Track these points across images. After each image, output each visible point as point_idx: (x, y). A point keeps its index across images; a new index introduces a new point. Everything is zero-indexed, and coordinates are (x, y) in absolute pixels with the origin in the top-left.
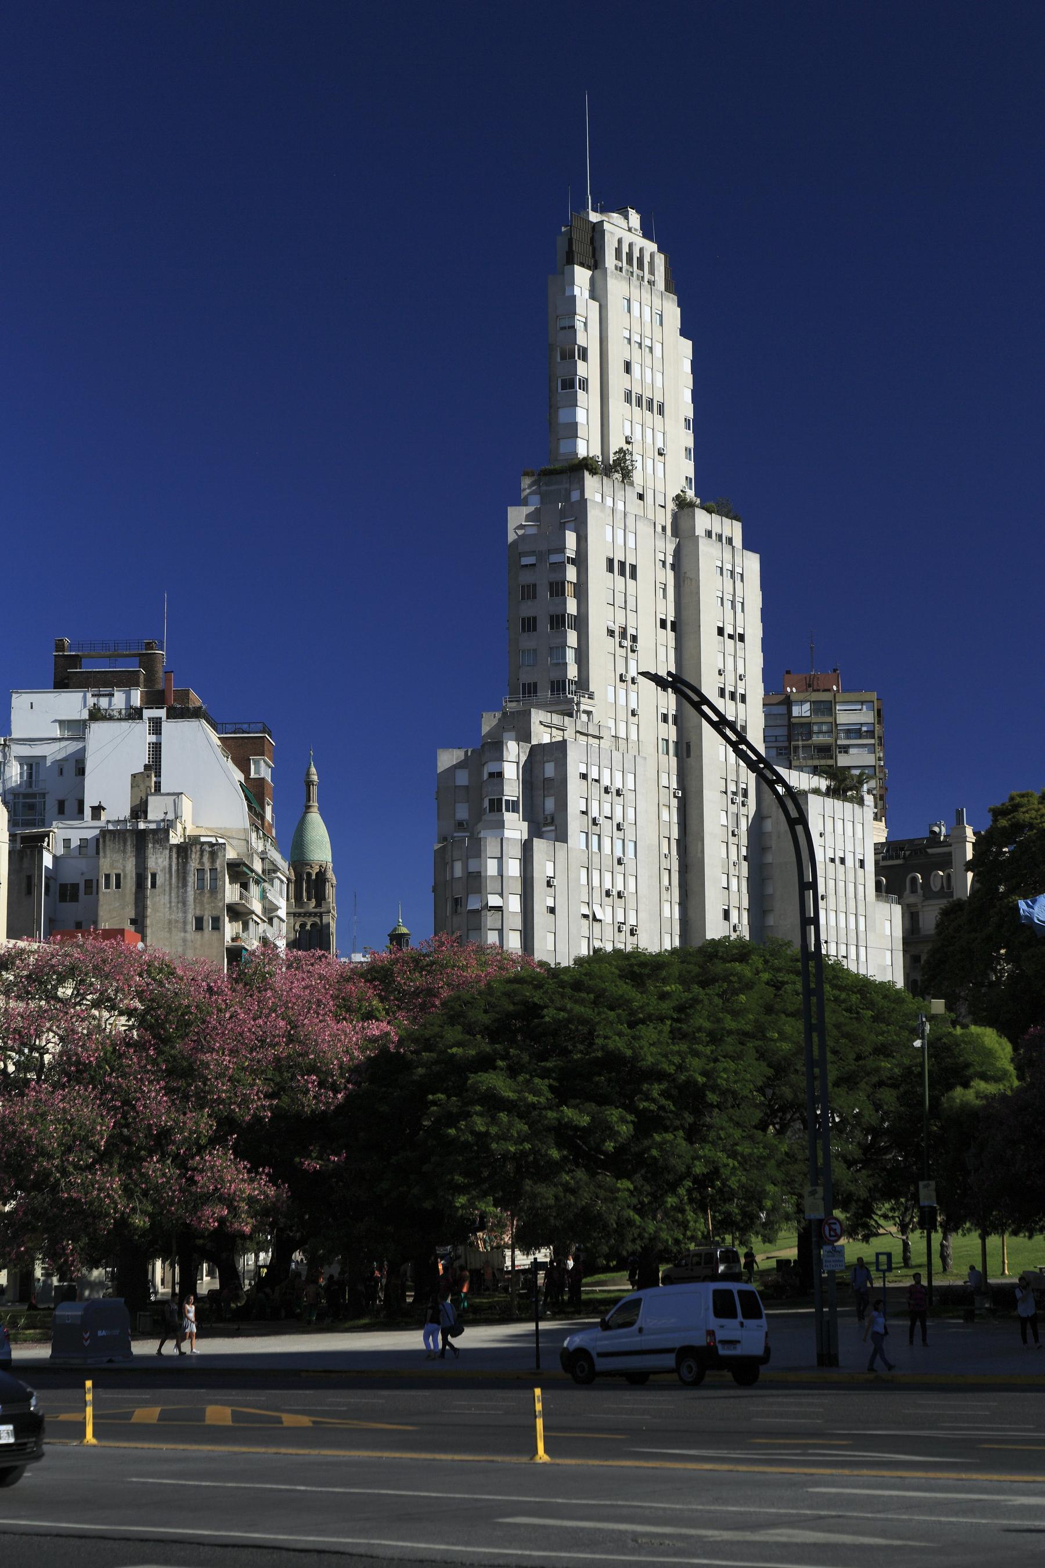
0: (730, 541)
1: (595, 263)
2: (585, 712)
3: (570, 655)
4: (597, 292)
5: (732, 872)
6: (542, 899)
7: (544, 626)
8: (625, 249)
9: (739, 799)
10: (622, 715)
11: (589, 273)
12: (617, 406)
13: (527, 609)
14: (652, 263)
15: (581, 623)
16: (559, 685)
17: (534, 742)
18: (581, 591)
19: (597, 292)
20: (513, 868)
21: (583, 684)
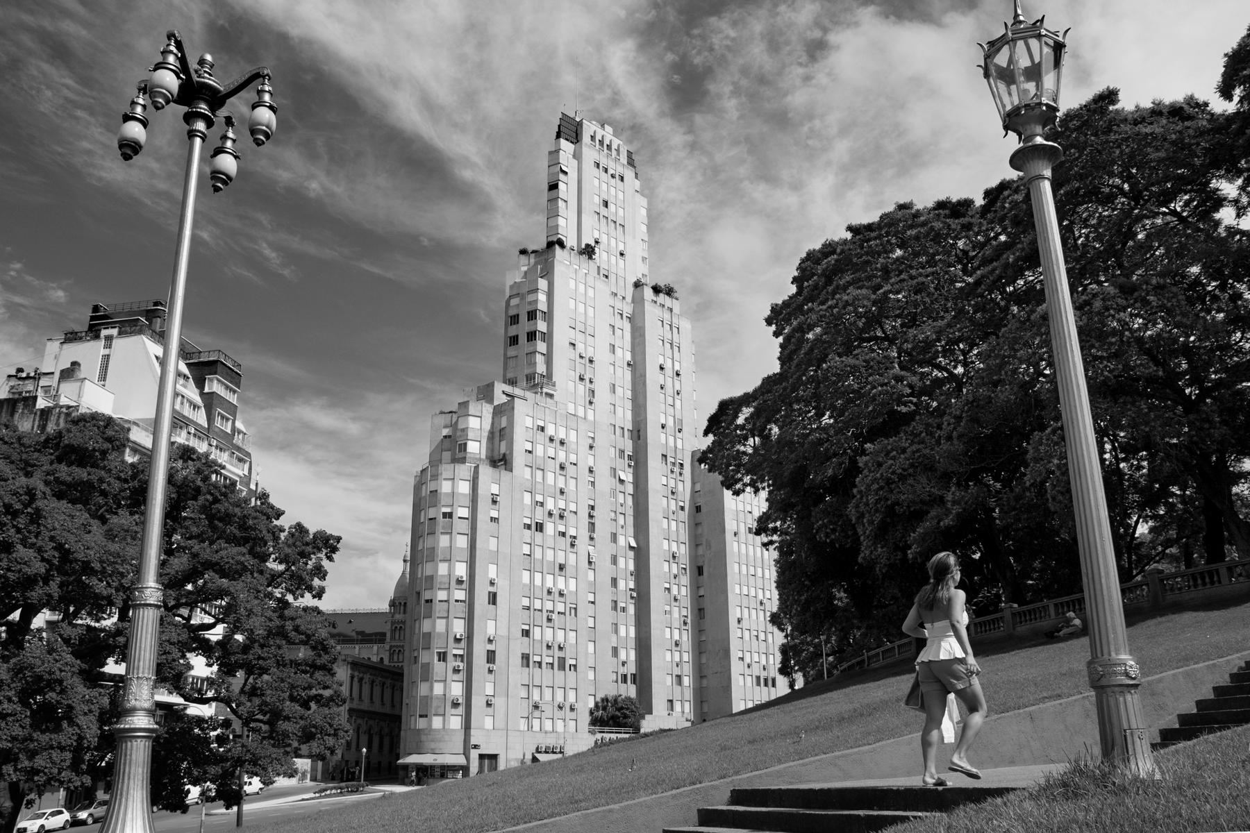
0: (671, 310)
1: (576, 138)
2: (547, 394)
3: (540, 359)
4: (577, 156)
5: (671, 516)
6: (486, 511)
7: (523, 339)
8: (598, 137)
9: (677, 469)
10: (581, 401)
11: (572, 146)
12: (588, 220)
13: (513, 331)
14: (618, 150)
15: (548, 337)
16: (530, 377)
17: (496, 403)
18: (548, 316)
19: (577, 156)
20: (464, 488)
21: (549, 376)
